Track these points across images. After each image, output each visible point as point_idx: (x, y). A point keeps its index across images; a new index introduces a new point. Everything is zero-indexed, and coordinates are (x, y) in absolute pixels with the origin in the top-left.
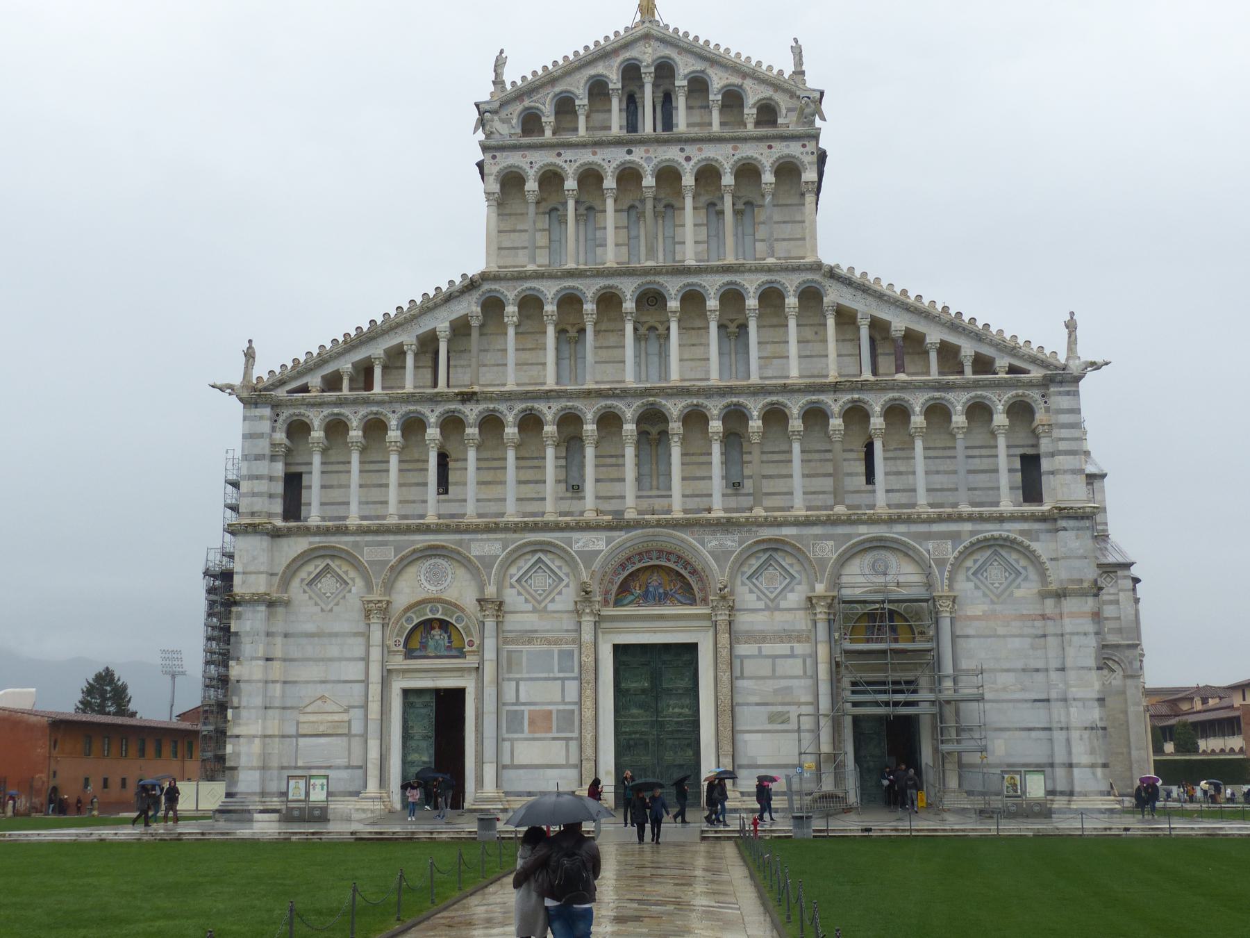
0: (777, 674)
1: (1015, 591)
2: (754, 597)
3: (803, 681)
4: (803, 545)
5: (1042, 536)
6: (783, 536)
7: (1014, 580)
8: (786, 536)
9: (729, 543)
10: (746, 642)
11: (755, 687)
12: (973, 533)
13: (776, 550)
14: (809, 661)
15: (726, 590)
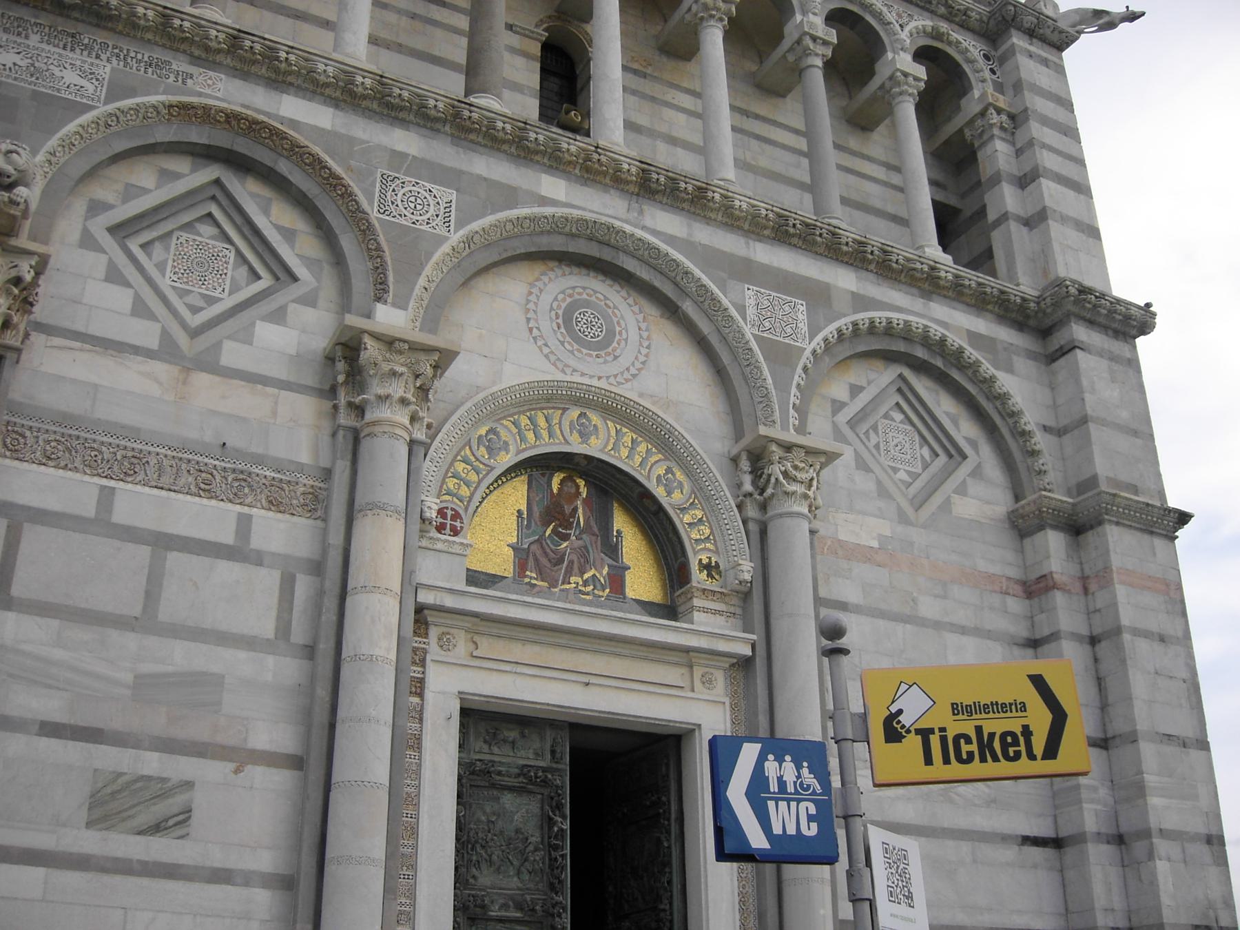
0: (166, 612)
1: (956, 498)
2: (121, 298)
3: (270, 660)
4: (349, 169)
5: (1021, 363)
6: (282, 120)
7: (946, 474)
8: (294, 123)
9: (71, 77)
10: (48, 459)
11: (58, 654)
12: (861, 303)
13: (243, 165)
14: (303, 587)
15: (21, 191)
